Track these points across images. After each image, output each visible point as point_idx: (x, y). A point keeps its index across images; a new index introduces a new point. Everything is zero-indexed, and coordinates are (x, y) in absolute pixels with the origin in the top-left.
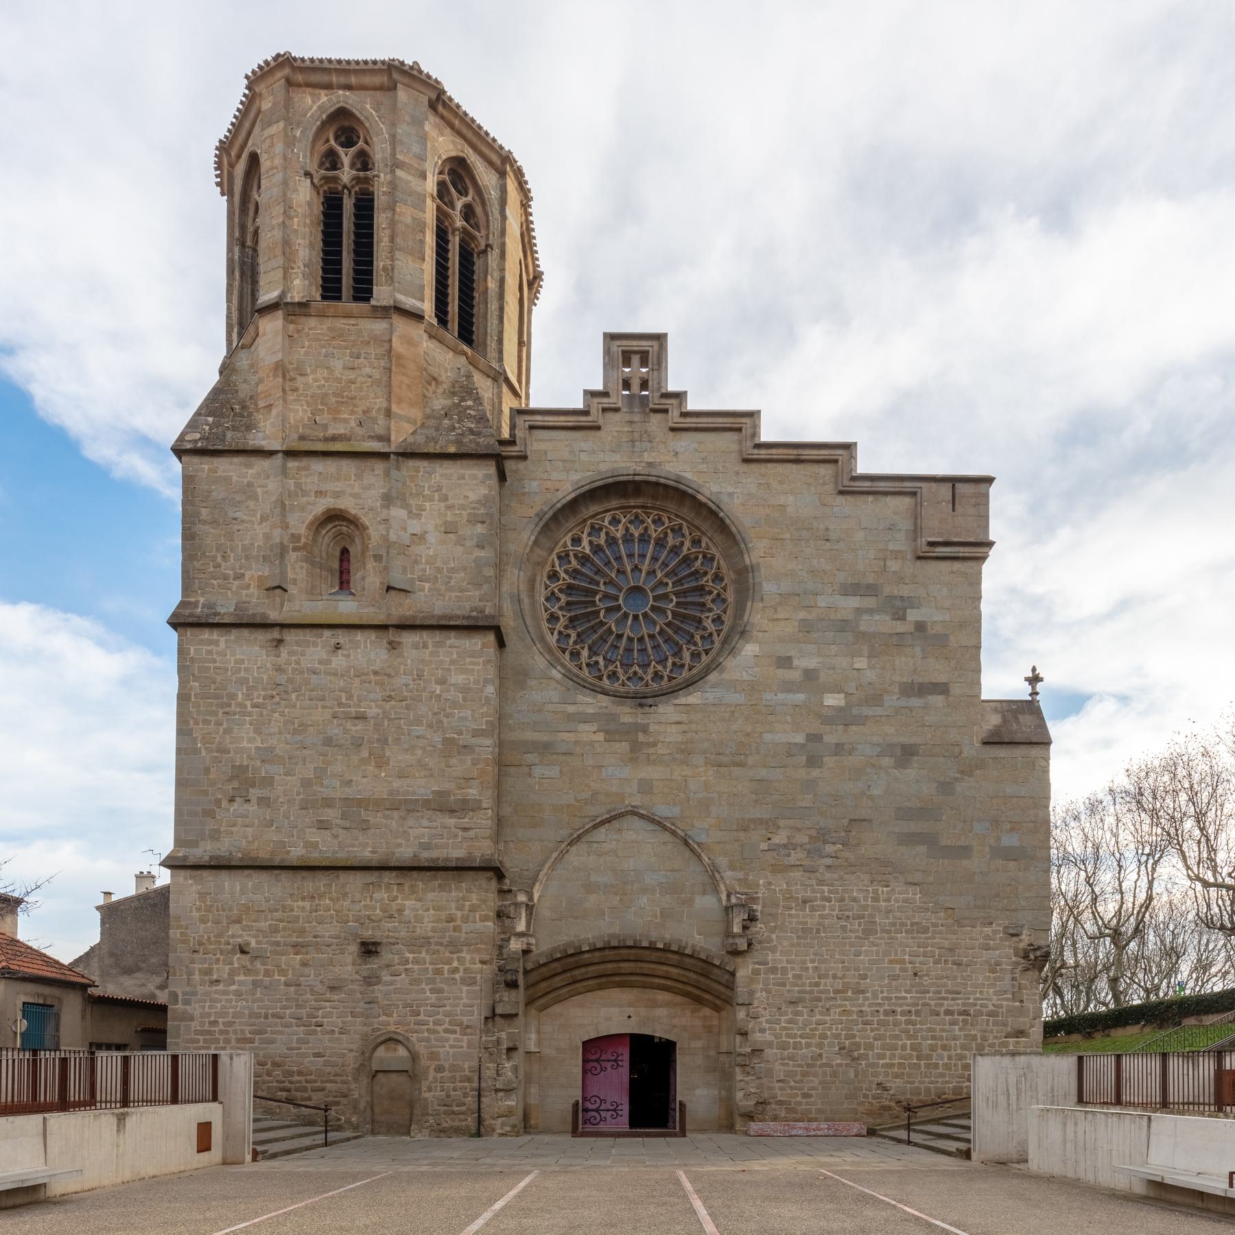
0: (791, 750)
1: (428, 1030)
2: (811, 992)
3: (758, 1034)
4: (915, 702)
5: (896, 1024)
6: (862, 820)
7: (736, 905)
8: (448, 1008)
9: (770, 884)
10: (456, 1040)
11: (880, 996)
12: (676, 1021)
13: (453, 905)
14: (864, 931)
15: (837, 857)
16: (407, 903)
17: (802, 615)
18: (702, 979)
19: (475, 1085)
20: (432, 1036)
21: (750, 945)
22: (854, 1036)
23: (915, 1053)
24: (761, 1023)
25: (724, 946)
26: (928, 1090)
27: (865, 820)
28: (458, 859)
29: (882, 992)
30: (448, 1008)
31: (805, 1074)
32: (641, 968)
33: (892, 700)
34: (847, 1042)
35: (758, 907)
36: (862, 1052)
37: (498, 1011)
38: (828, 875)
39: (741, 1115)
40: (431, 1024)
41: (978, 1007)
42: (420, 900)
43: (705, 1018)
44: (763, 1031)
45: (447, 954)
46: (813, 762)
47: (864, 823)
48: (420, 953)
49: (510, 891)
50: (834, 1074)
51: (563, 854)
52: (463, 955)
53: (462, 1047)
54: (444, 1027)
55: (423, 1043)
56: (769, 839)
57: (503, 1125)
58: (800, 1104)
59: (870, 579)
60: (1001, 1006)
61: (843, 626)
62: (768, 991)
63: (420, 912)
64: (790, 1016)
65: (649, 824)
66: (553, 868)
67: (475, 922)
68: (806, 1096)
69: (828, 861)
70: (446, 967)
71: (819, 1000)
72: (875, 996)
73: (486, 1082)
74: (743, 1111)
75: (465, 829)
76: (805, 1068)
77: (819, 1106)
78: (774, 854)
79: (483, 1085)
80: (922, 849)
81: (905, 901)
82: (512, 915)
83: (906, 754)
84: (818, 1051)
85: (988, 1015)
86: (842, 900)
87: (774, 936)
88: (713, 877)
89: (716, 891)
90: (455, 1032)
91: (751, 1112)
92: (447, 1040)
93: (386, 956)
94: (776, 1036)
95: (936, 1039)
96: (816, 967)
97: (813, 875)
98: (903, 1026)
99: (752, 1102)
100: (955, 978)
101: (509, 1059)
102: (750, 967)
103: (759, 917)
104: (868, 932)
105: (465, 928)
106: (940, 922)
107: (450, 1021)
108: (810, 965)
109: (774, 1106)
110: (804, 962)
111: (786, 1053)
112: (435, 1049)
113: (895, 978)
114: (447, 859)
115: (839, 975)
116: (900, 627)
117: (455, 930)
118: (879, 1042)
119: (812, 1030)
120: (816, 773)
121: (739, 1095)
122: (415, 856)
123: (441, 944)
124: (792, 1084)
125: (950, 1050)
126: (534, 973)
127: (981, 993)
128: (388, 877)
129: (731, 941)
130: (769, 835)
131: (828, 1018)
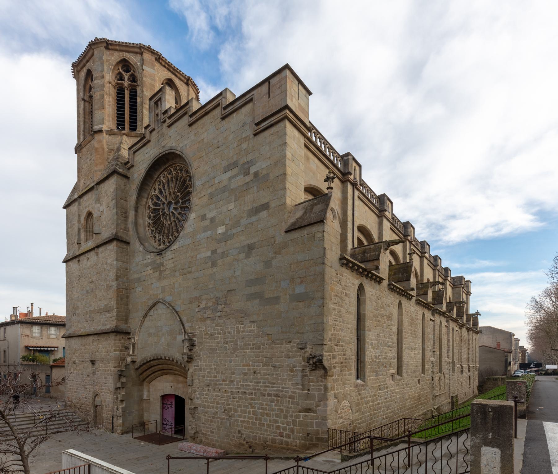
23: (254, 417)
24: (196, 394)
26: (260, 438)
29: (240, 382)
31: (212, 421)
34: (227, 407)
36: (233, 413)
41: (284, 393)
44: (198, 398)
46: (214, 264)
50: (222, 423)
58: (209, 435)
60: (295, 393)
62: (199, 380)
68: (212, 432)
71: (216, 384)
72: (237, 384)
77: (216, 438)
80: (257, 301)
84: (216, 411)
85: (289, 398)
86: (225, 333)
95: (264, 410)
98: (249, 401)
100: (273, 374)
106: (265, 342)
108: (213, 367)
109: (201, 435)
110: (211, 366)
115: (223, 372)
120: (215, 269)
124: (207, 425)
125: (270, 417)
127: (285, 384)
131: (220, 394)
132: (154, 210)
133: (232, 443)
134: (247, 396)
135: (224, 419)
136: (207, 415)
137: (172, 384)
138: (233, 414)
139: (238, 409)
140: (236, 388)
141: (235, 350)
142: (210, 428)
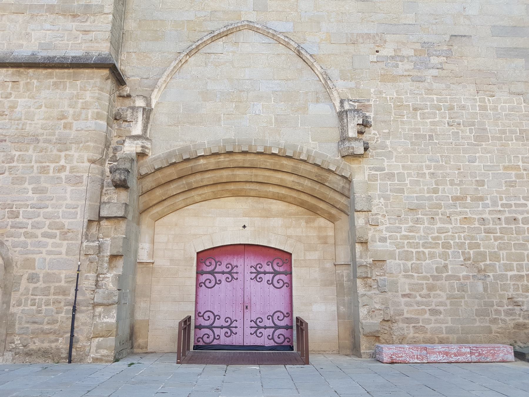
1: (26, 234)
2: (430, 199)
3: (379, 243)
5: (519, 232)
6: (462, 36)
7: (350, 110)
8: (50, 209)
9: (381, 93)
10: (55, 245)
11: (500, 203)
12: (290, 232)
13: (66, 102)
14: (476, 138)
15: (442, 69)
16: (19, 100)
18: (317, 187)
19: (71, 297)
20: (29, 241)
21: (366, 149)
22: (478, 246)
25: (339, 151)
27: (465, 36)
28: (74, 57)
29: (501, 199)
30: (50, 209)
31: (431, 288)
32: (256, 176)
34: (471, 252)
35: (371, 115)
36: (488, 262)
37: (104, 213)
38: (435, 85)
39: (366, 335)
40: (30, 227)
42: (33, 97)
43: (320, 228)
44: (383, 240)
45: (55, 152)
47: (464, 39)
48: (27, 150)
49: (129, 96)
50: (462, 288)
51: (182, 63)
52: (72, 153)
53: (60, 254)
54: (43, 230)
55: (18, 249)
56: (377, 52)
57: (99, 347)
58: (429, 321)
62: (387, 198)
63: (32, 109)
64: (411, 224)
65: (264, 37)
66: (172, 75)
67: (87, 119)
68: (434, 312)
69: (435, 72)
70: (52, 166)
71: (439, 206)
72: (495, 204)
73: (84, 294)
74: (367, 330)
75: (86, 32)
76: (431, 281)
77: (450, 324)
78: (382, 65)
79: (79, 298)
81: (512, 109)
82: (128, 119)
84: (443, 262)
86: (451, 108)
87: (388, 142)
88: (326, 86)
89: (329, 98)
90: (54, 236)
91: (378, 331)
92: (45, 245)
94: (398, 246)
96: (433, 174)
97: (421, 84)
99: (377, 320)
101: (111, 267)
102: (367, 173)
103: (372, 123)
104: (481, 138)
105: (76, 125)
107: (50, 224)
108: (427, 172)
109: (401, 325)
111: (409, 263)
112: (30, 256)
113: (511, 184)
114: (64, 58)
115: (457, 181)
117: (65, 127)
118: (505, 252)
119: (434, 238)
121: (363, 312)
122: (33, 54)
123: (49, 141)
124: (419, 298)
126: (149, 179)
129: (347, 144)
130: (377, 49)
131: (449, 226)
133: (494, 327)
134: (521, 225)
135: (467, 277)
136: (416, 275)
137: (246, 221)
138: (489, 265)
139: (501, 252)
140: (491, 213)
142: (427, 304)
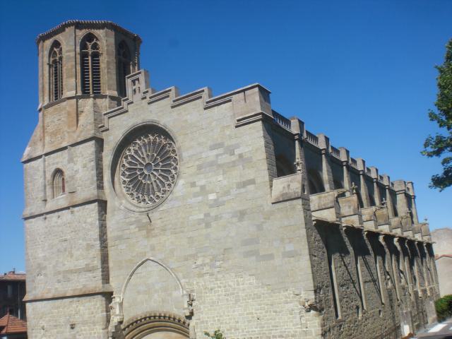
0: (200, 222)
4: (243, 190)
17: (197, 163)
33: (234, 192)
59: (220, 141)
60: (296, 332)
61: (212, 164)
69: (218, 269)
72: (243, 331)
80: (254, 258)
83: (242, 215)
86: (225, 287)
87: (202, 307)
93: (77, 328)
100: (275, 319)
104: (237, 301)
110: (214, 317)
115: (228, 322)
116: (233, 158)
120: (209, 230)
128: (75, 299)
132: (129, 169)
141: (237, 301)
